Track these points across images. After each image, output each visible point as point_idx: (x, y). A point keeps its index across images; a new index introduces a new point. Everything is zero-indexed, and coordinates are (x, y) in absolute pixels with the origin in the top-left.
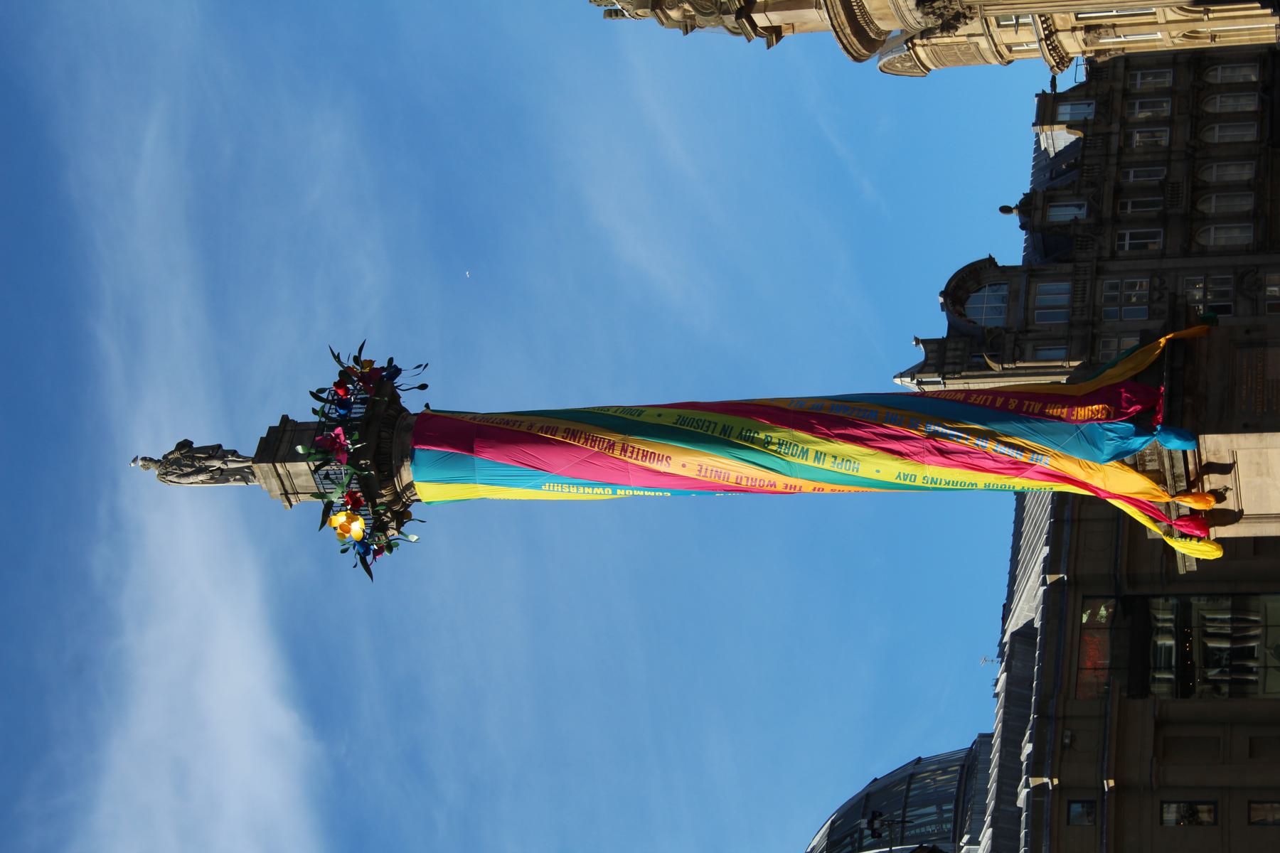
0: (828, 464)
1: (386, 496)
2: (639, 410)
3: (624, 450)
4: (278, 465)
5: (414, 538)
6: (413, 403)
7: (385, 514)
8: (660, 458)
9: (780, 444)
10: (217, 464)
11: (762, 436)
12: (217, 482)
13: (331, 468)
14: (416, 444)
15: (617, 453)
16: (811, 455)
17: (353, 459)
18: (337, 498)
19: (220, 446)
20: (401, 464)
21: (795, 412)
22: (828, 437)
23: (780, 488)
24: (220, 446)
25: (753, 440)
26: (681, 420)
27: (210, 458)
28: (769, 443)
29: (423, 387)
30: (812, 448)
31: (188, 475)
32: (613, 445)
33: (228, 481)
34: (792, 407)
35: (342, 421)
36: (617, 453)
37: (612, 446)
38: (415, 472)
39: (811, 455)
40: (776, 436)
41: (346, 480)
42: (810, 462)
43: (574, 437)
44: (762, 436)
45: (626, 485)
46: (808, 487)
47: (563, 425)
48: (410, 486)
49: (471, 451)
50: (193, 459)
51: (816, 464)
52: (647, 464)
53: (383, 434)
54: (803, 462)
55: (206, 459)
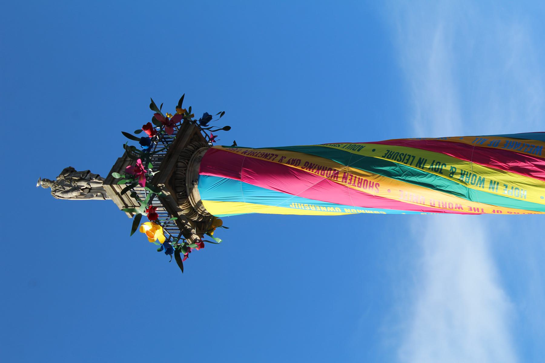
0: (501, 191)
1: (183, 211)
2: (359, 146)
3: (345, 178)
4: (115, 186)
5: (219, 241)
6: (222, 141)
7: (186, 223)
8: (371, 185)
9: (462, 174)
10: (84, 184)
11: (448, 168)
12: (86, 197)
13: (138, 189)
14: (201, 172)
15: (340, 180)
16: (487, 185)
17: (152, 184)
18: (141, 210)
19: (89, 172)
20: (194, 187)
21: (477, 148)
22: (502, 169)
23: (466, 210)
24: (89, 172)
25: (441, 171)
26: (389, 154)
27: (81, 180)
28: (453, 173)
29: (227, 128)
30: (488, 178)
31: (67, 192)
32: (338, 173)
33: (92, 196)
34: (475, 144)
35: (146, 156)
36: (340, 180)
37: (336, 175)
38: (201, 193)
39: (487, 185)
40: (459, 167)
41: (147, 199)
42: (486, 190)
43: (311, 167)
44: (448, 168)
45: (350, 205)
46: (488, 209)
47: (305, 159)
48: (200, 203)
49: (238, 177)
50: (71, 180)
51: (491, 191)
52: (362, 189)
53: (180, 164)
54: (481, 189)
55: (78, 181)
